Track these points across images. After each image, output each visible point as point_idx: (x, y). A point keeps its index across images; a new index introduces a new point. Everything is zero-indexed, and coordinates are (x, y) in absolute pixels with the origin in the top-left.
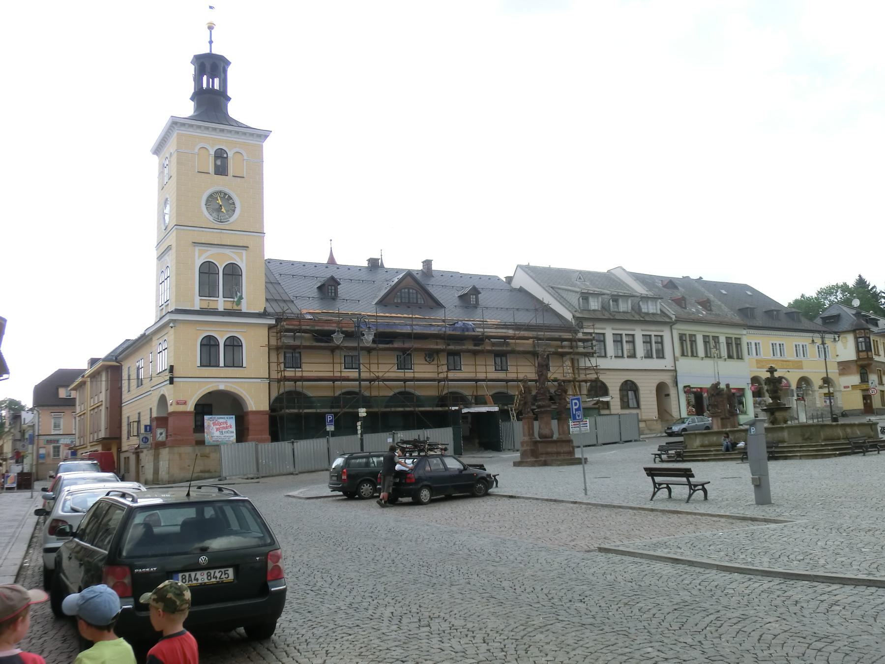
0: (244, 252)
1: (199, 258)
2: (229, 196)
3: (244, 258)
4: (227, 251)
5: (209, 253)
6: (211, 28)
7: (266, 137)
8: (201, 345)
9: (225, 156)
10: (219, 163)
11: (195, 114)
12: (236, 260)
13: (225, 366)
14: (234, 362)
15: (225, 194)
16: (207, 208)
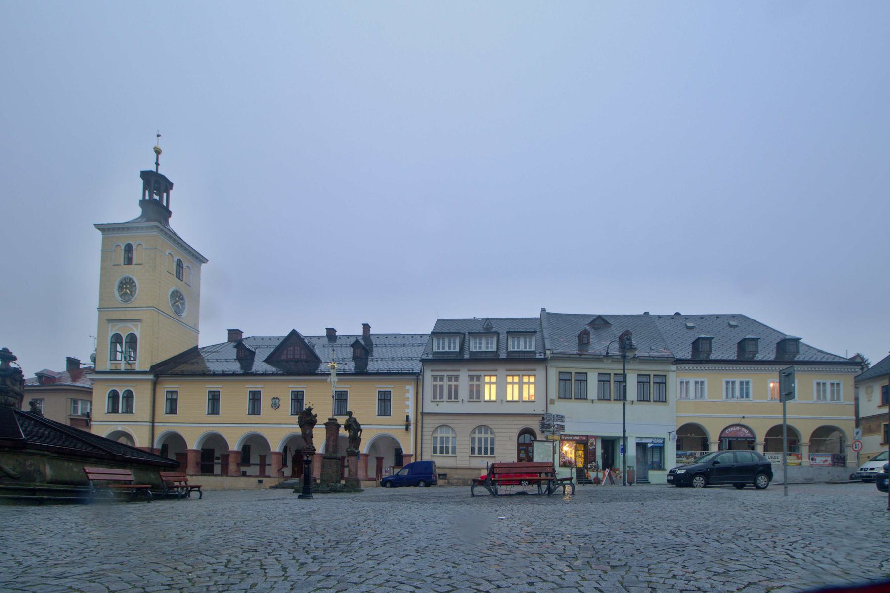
0: (140, 324)
1: (111, 331)
3: (139, 328)
6: (158, 152)
15: (130, 279)
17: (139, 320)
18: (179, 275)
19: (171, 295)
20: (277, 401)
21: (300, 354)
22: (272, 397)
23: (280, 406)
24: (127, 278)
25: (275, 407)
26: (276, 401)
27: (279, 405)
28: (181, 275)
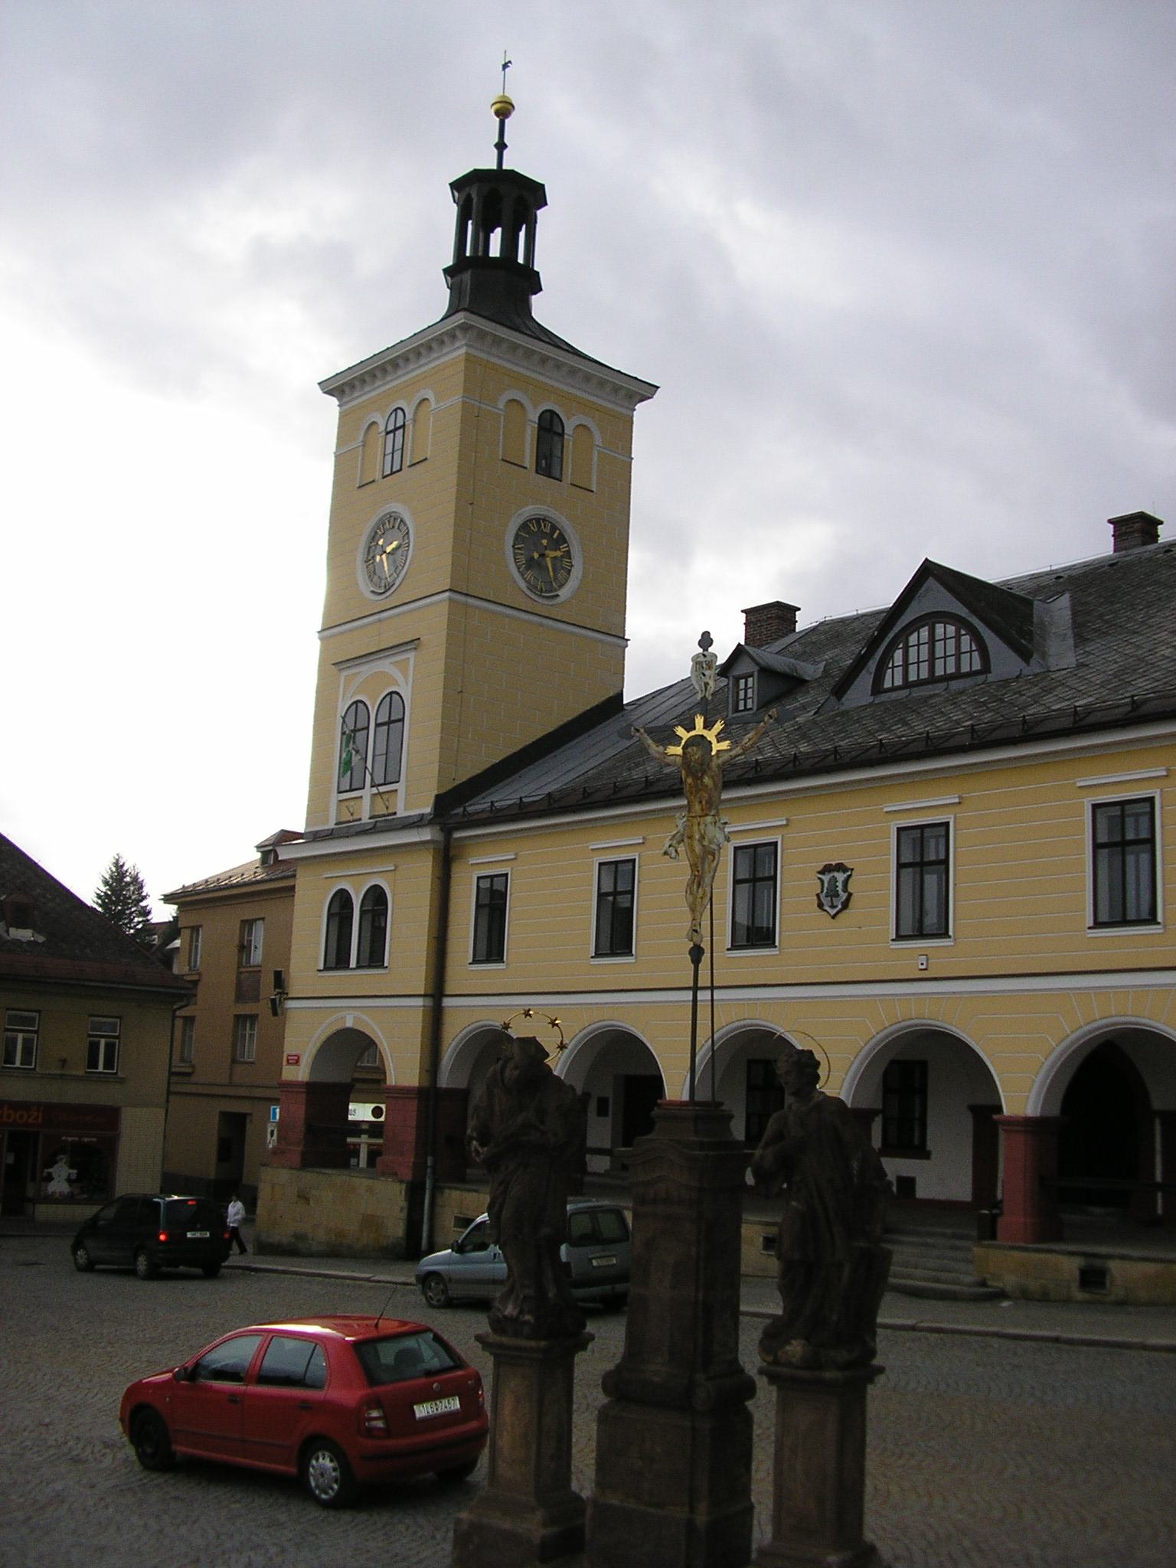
12: (399, 685)
13: (359, 967)
14: (374, 957)
17: (414, 643)
18: (548, 462)
19: (517, 537)
20: (840, 877)
21: (958, 655)
22: (820, 867)
25: (833, 907)
27: (850, 895)
28: (556, 461)
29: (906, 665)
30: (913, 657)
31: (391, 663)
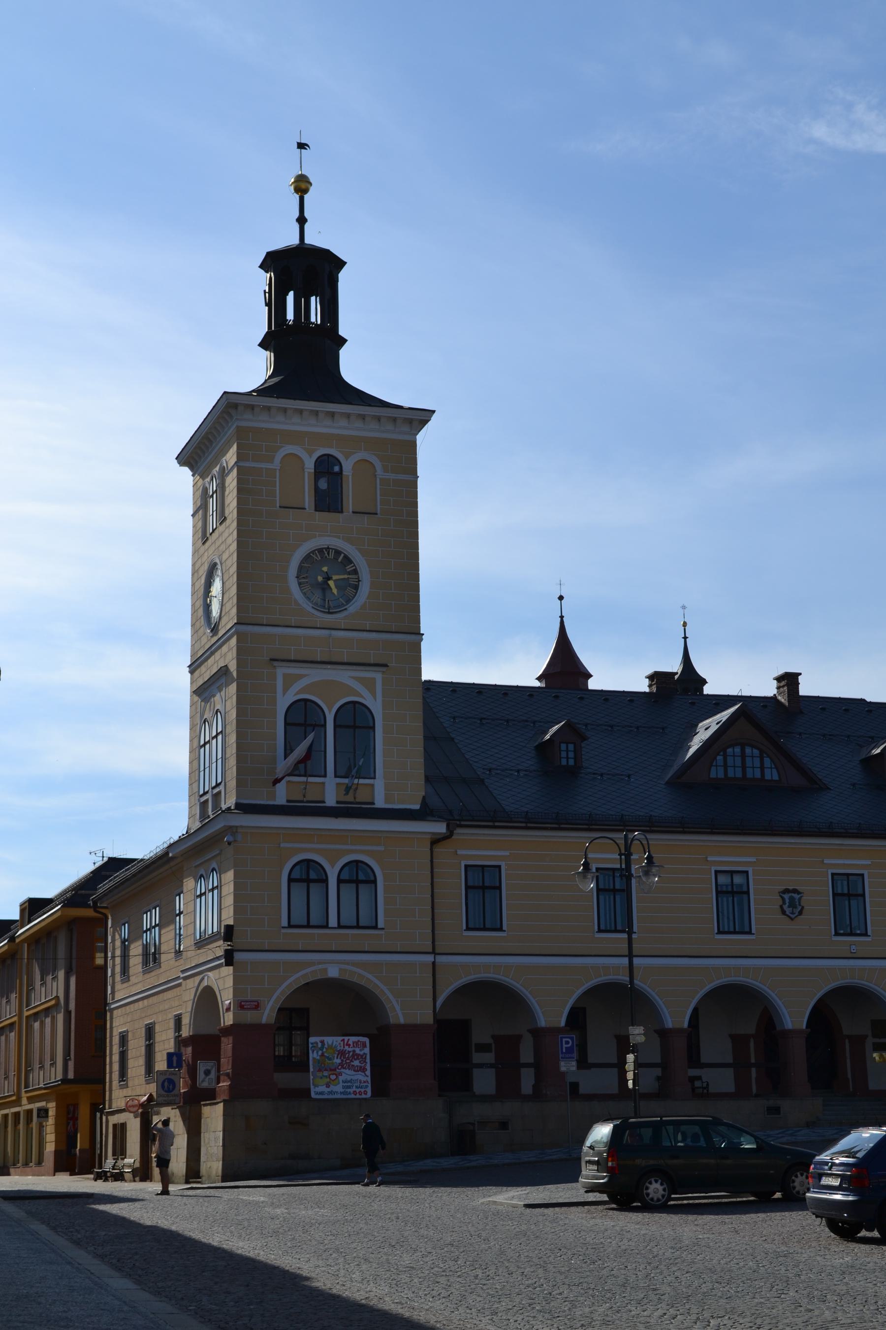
1: (285, 691)
2: (346, 557)
4: (344, 676)
5: (303, 683)
7: (424, 422)
8: (290, 880)
9: (337, 469)
10: (323, 484)
11: (275, 380)
12: (362, 697)
16: (300, 584)
20: (796, 896)
23: (804, 911)
24: (328, 549)
25: (793, 913)
26: (792, 899)
27: (803, 908)
29: (725, 766)
30: (730, 761)
31: (352, 677)
